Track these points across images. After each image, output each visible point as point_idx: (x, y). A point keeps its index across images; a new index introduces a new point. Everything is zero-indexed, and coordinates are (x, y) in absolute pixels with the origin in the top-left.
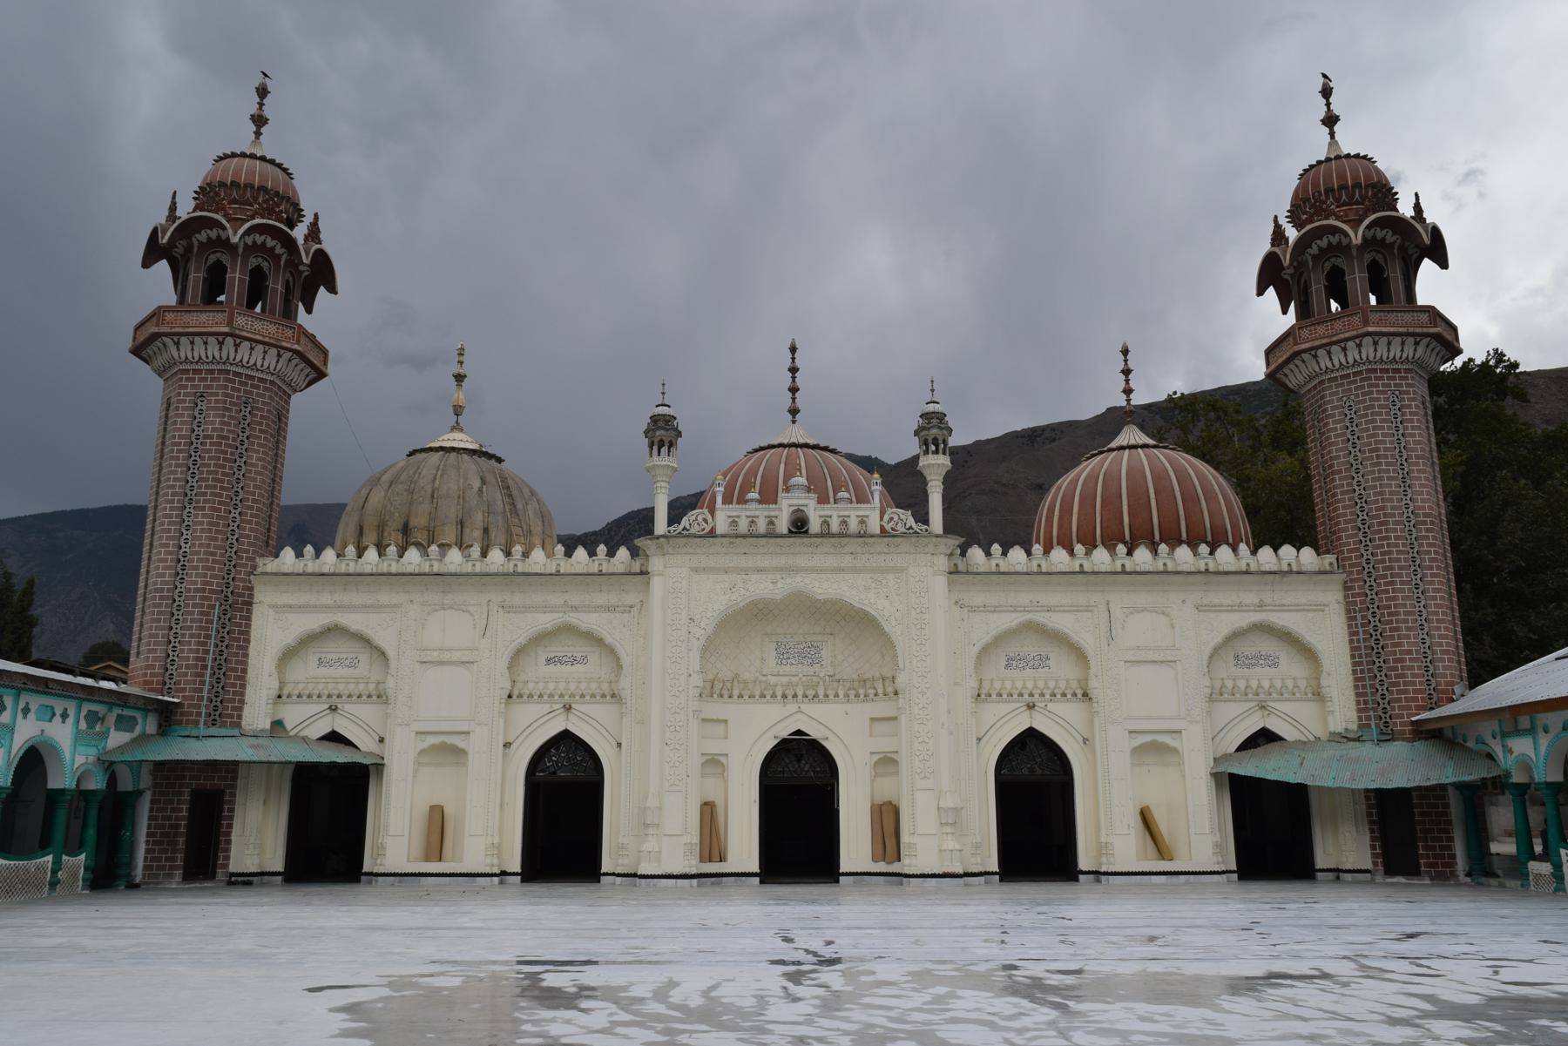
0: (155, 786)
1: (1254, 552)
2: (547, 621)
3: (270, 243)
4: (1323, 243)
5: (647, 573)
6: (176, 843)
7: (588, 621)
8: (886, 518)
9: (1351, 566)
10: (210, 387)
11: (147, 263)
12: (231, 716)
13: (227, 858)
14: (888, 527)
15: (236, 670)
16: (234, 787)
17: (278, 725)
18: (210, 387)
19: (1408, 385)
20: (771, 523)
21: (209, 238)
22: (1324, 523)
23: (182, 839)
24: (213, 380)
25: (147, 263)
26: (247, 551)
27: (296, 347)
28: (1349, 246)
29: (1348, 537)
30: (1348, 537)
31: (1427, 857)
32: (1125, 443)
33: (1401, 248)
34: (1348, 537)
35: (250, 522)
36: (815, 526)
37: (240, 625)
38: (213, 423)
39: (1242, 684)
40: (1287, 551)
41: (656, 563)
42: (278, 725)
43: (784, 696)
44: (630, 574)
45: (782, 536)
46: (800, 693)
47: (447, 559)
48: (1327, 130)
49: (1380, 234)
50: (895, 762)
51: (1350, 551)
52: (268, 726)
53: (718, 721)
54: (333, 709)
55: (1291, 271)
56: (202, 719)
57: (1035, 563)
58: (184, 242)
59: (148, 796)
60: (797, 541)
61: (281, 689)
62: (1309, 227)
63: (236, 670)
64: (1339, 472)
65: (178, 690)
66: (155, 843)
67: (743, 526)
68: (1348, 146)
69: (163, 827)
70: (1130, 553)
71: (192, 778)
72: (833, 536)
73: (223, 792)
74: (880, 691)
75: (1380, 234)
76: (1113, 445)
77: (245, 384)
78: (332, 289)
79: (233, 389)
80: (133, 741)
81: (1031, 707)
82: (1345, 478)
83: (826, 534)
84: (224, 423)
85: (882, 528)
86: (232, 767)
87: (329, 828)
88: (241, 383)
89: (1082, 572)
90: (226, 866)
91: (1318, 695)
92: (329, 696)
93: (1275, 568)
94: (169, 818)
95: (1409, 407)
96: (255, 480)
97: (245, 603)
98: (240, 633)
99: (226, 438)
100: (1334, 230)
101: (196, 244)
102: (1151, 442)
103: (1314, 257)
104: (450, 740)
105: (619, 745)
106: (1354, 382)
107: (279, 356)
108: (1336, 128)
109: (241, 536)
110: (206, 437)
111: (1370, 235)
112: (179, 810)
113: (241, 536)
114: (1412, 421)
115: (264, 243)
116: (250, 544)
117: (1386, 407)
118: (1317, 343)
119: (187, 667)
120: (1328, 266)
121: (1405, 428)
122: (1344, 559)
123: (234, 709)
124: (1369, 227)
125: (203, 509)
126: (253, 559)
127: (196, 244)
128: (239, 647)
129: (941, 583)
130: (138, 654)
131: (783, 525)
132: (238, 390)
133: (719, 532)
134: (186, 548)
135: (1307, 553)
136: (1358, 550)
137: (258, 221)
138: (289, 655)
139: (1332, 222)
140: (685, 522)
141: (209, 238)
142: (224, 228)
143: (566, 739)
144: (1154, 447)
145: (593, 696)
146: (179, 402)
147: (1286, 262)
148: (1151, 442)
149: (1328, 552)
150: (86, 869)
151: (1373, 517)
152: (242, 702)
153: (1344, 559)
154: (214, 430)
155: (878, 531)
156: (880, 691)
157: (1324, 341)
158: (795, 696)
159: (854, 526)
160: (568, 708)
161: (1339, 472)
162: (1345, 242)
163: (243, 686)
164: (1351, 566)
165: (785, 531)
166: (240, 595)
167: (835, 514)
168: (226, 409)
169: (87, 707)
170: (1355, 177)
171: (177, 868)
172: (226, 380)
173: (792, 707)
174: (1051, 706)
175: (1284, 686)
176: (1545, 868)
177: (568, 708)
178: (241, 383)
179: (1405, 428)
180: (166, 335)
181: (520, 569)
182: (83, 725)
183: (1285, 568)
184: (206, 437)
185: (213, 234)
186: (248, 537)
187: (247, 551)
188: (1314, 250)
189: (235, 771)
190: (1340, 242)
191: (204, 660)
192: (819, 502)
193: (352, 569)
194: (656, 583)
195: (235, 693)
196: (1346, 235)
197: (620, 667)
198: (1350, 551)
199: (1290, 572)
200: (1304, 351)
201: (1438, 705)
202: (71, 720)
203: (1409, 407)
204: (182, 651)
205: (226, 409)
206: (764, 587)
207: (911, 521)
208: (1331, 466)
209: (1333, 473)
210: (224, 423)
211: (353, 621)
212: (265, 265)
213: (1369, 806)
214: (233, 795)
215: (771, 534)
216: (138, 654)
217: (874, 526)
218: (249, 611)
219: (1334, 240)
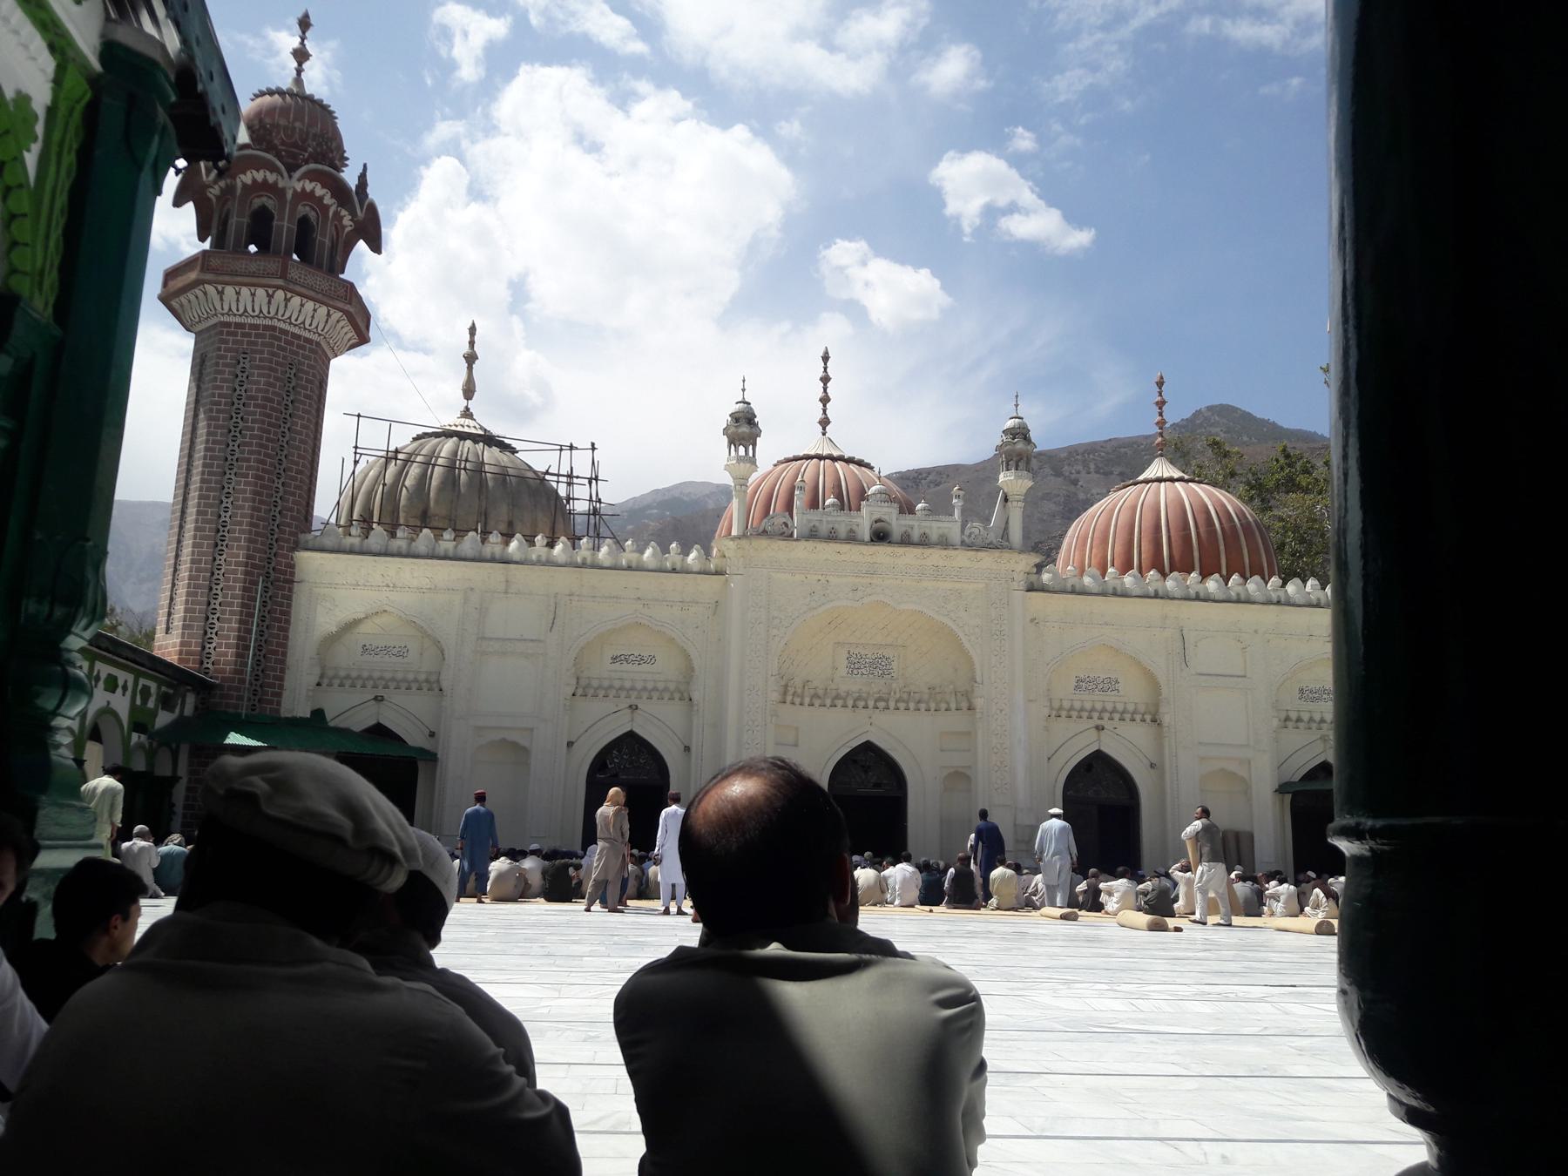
3: (319, 191)
10: (255, 344)
15: (276, 652)
18: (255, 344)
21: (254, 181)
26: (289, 525)
27: (347, 307)
32: (1152, 476)
35: (293, 494)
38: (258, 383)
39: (1306, 717)
45: (862, 542)
50: (968, 778)
54: (378, 699)
61: (322, 676)
74: (953, 706)
76: (1141, 478)
77: (292, 344)
79: (280, 348)
81: (1099, 728)
84: (269, 384)
96: (298, 448)
99: (272, 401)
101: (239, 184)
102: (1177, 474)
105: (687, 749)
109: (284, 508)
113: (284, 508)
115: (313, 191)
125: (246, 476)
126: (295, 535)
127: (239, 184)
128: (280, 629)
132: (284, 349)
134: (226, 517)
137: (312, 166)
141: (254, 181)
144: (1180, 480)
148: (1177, 474)
152: (281, 687)
154: (258, 390)
156: (953, 706)
163: (283, 671)
165: (867, 537)
166: (280, 572)
167: (916, 524)
168: (271, 369)
172: (272, 337)
178: (287, 342)
187: (289, 525)
192: (901, 512)
204: (222, 629)
205: (271, 369)
210: (269, 384)
212: (312, 215)
215: (852, 538)
218: (290, 590)
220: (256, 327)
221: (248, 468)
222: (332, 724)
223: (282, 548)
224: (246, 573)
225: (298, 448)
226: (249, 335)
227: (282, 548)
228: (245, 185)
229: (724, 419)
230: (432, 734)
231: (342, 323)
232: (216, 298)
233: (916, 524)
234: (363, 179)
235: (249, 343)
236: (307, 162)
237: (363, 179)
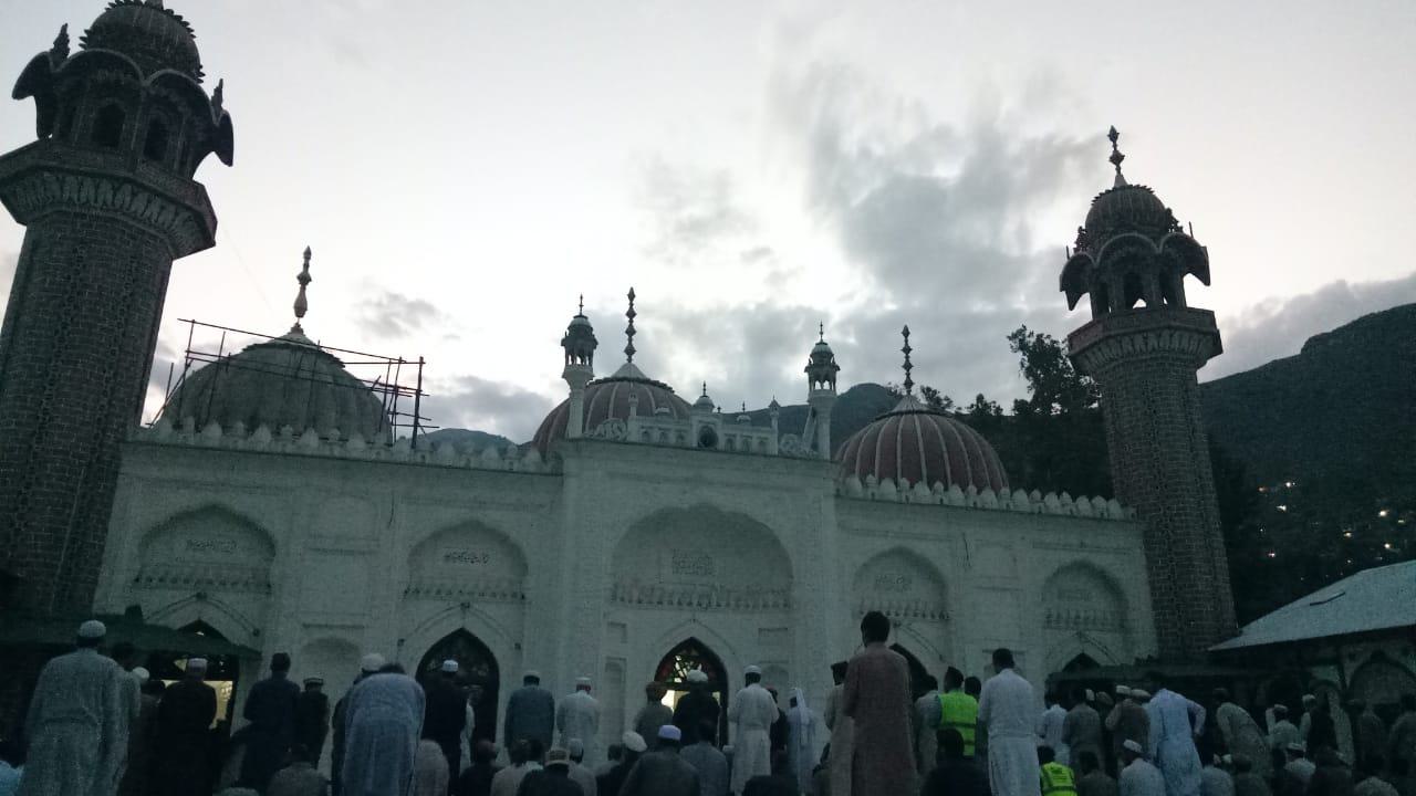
1: (1074, 499)
2: (448, 515)
5: (562, 475)
7: (492, 517)
8: (783, 441)
14: (784, 450)
17: (134, 611)
20: (682, 437)
25: (19, 93)
36: (722, 443)
40: (1099, 501)
41: (570, 465)
42: (134, 611)
43: (680, 603)
44: (541, 474)
46: (695, 602)
47: (349, 445)
48: (1114, 166)
52: (122, 611)
53: (618, 624)
54: (200, 597)
57: (869, 493)
60: (702, 455)
67: (656, 436)
68: (1132, 179)
70: (979, 492)
72: (754, 454)
83: (731, 451)
85: (780, 451)
89: (975, 508)
91: (1123, 627)
92: (198, 582)
93: (1091, 515)
104: (340, 634)
105: (518, 647)
107: (177, 214)
108: (1121, 165)
129: (829, 505)
131: (693, 439)
138: (155, 533)
139: (1136, 234)
140: (600, 428)
143: (462, 634)
145: (494, 595)
155: (777, 453)
158: (690, 604)
159: (755, 444)
160: (465, 606)
165: (695, 445)
167: (738, 433)
173: (687, 615)
174: (915, 626)
175: (1078, 617)
177: (465, 606)
180: (50, 169)
181: (428, 461)
183: (1098, 516)
193: (241, 444)
194: (572, 484)
197: (525, 567)
201: (1223, 640)
206: (672, 496)
211: (239, 503)
217: (773, 448)
222: (149, 622)
229: (562, 330)
230: (256, 633)
232: (55, 187)
233: (738, 433)
234: (219, 91)
237: (219, 91)
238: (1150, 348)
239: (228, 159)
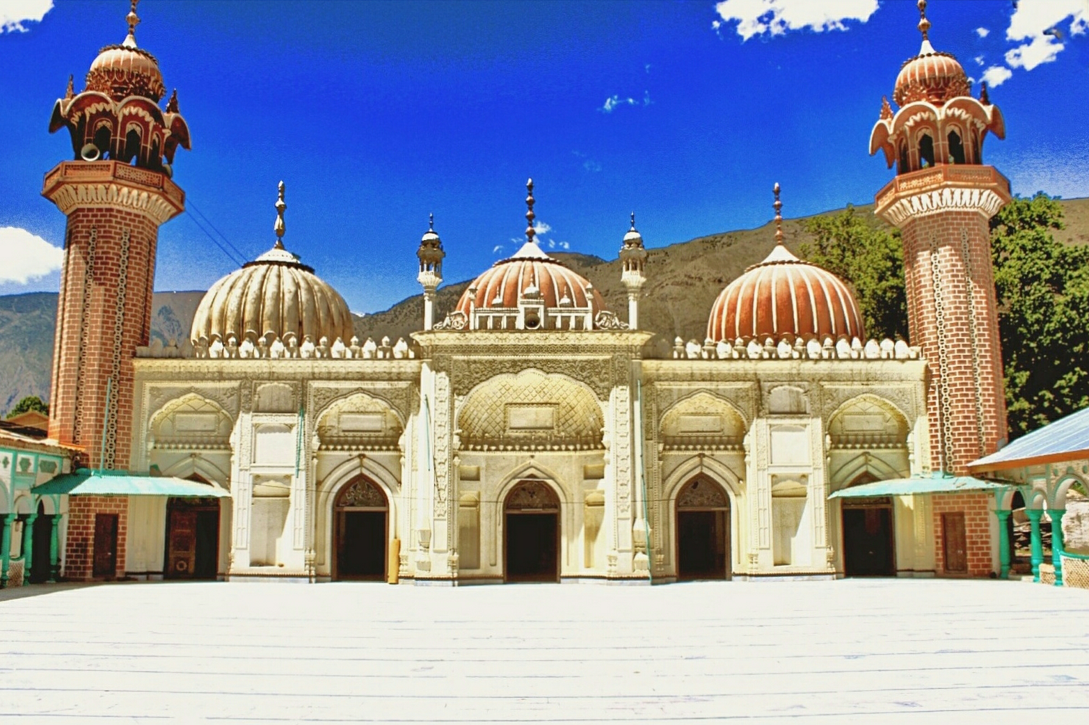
0: (71, 511)
4: (918, 118)
6: (85, 551)
8: (597, 317)
9: (931, 355)
11: (52, 130)
12: (122, 462)
13: (123, 562)
15: (123, 428)
16: (124, 512)
18: (100, 221)
19: (974, 224)
22: (913, 323)
23: (91, 549)
24: (102, 216)
25: (52, 130)
28: (935, 121)
29: (929, 334)
30: (930, 334)
31: (973, 560)
33: (973, 124)
34: (930, 334)
35: (130, 320)
37: (125, 396)
40: (887, 344)
49: (957, 112)
51: (931, 344)
55: (895, 137)
56: (101, 464)
58: (79, 113)
59: (66, 519)
62: (907, 106)
63: (123, 428)
64: (925, 286)
65: (84, 443)
66: (73, 551)
69: (76, 540)
71: (96, 505)
73: (114, 518)
75: (957, 112)
77: (125, 219)
78: (186, 146)
80: (55, 478)
82: (929, 291)
86: (124, 498)
87: (195, 542)
88: (122, 218)
90: (122, 567)
94: (81, 534)
95: (975, 240)
96: (133, 289)
97: (128, 380)
98: (126, 401)
100: (925, 109)
103: (911, 128)
106: (937, 221)
109: (124, 331)
110: (98, 258)
111: (950, 112)
112: (86, 528)
114: (976, 250)
116: (131, 337)
117: (959, 239)
118: (911, 192)
119: (90, 426)
120: (920, 134)
121: (971, 256)
122: (926, 350)
123: (123, 456)
124: (950, 107)
128: (125, 412)
130: (55, 416)
132: (120, 223)
133: (471, 328)
135: (901, 344)
136: (937, 343)
137: (132, 97)
140: (447, 320)
142: (107, 102)
146: (78, 232)
147: (891, 131)
149: (915, 344)
150: (26, 569)
151: (946, 320)
153: (926, 350)
157: (917, 190)
161: (925, 286)
162: (932, 118)
164: (931, 355)
166: (124, 374)
169: (21, 456)
170: (941, 70)
171: (89, 568)
176: (1050, 568)
178: (122, 218)
179: (971, 256)
182: (19, 469)
184: (98, 258)
185: (100, 107)
186: (129, 331)
187: (129, 342)
188: (911, 123)
189: (125, 501)
190: (929, 118)
191: (101, 421)
195: (124, 445)
196: (933, 113)
198: (931, 344)
199: (888, 358)
200: (903, 197)
202: (10, 466)
203: (975, 240)
207: (616, 321)
208: (920, 282)
209: (921, 287)
213: (936, 526)
214: (125, 517)
216: (55, 416)
219: (925, 116)
220: (100, 210)
221: (98, 306)
223: (124, 358)
224: (100, 377)
225: (133, 289)
226: (96, 216)
227: (124, 358)
228: (91, 114)
231: (161, 201)
235: (97, 221)
236: (128, 95)
238: (935, 206)
239: (186, 146)
